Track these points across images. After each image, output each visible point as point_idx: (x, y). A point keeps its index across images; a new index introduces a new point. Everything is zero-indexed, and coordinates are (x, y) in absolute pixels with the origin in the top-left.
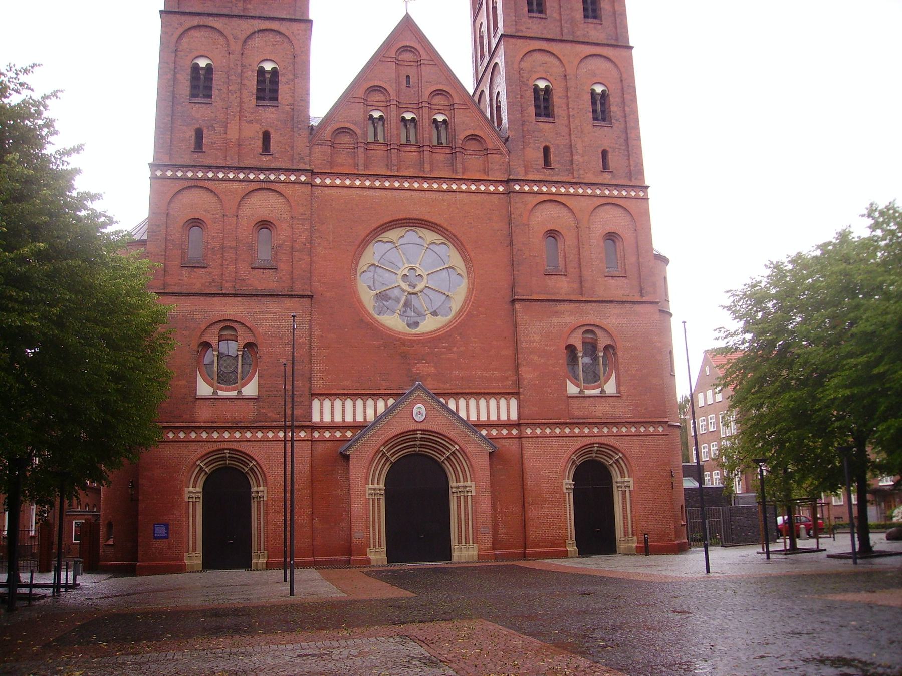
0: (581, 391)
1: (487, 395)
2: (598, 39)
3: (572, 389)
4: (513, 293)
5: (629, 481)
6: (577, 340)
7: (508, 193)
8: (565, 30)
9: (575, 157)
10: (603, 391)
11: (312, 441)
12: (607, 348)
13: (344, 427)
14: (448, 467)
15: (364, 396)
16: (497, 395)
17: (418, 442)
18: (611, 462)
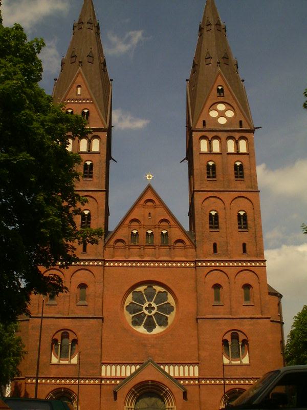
0: (230, 362)
1: (184, 364)
3: (226, 361)
6: (228, 337)
7: (196, 267)
10: (241, 362)
11: (101, 385)
13: (116, 379)
16: (189, 364)
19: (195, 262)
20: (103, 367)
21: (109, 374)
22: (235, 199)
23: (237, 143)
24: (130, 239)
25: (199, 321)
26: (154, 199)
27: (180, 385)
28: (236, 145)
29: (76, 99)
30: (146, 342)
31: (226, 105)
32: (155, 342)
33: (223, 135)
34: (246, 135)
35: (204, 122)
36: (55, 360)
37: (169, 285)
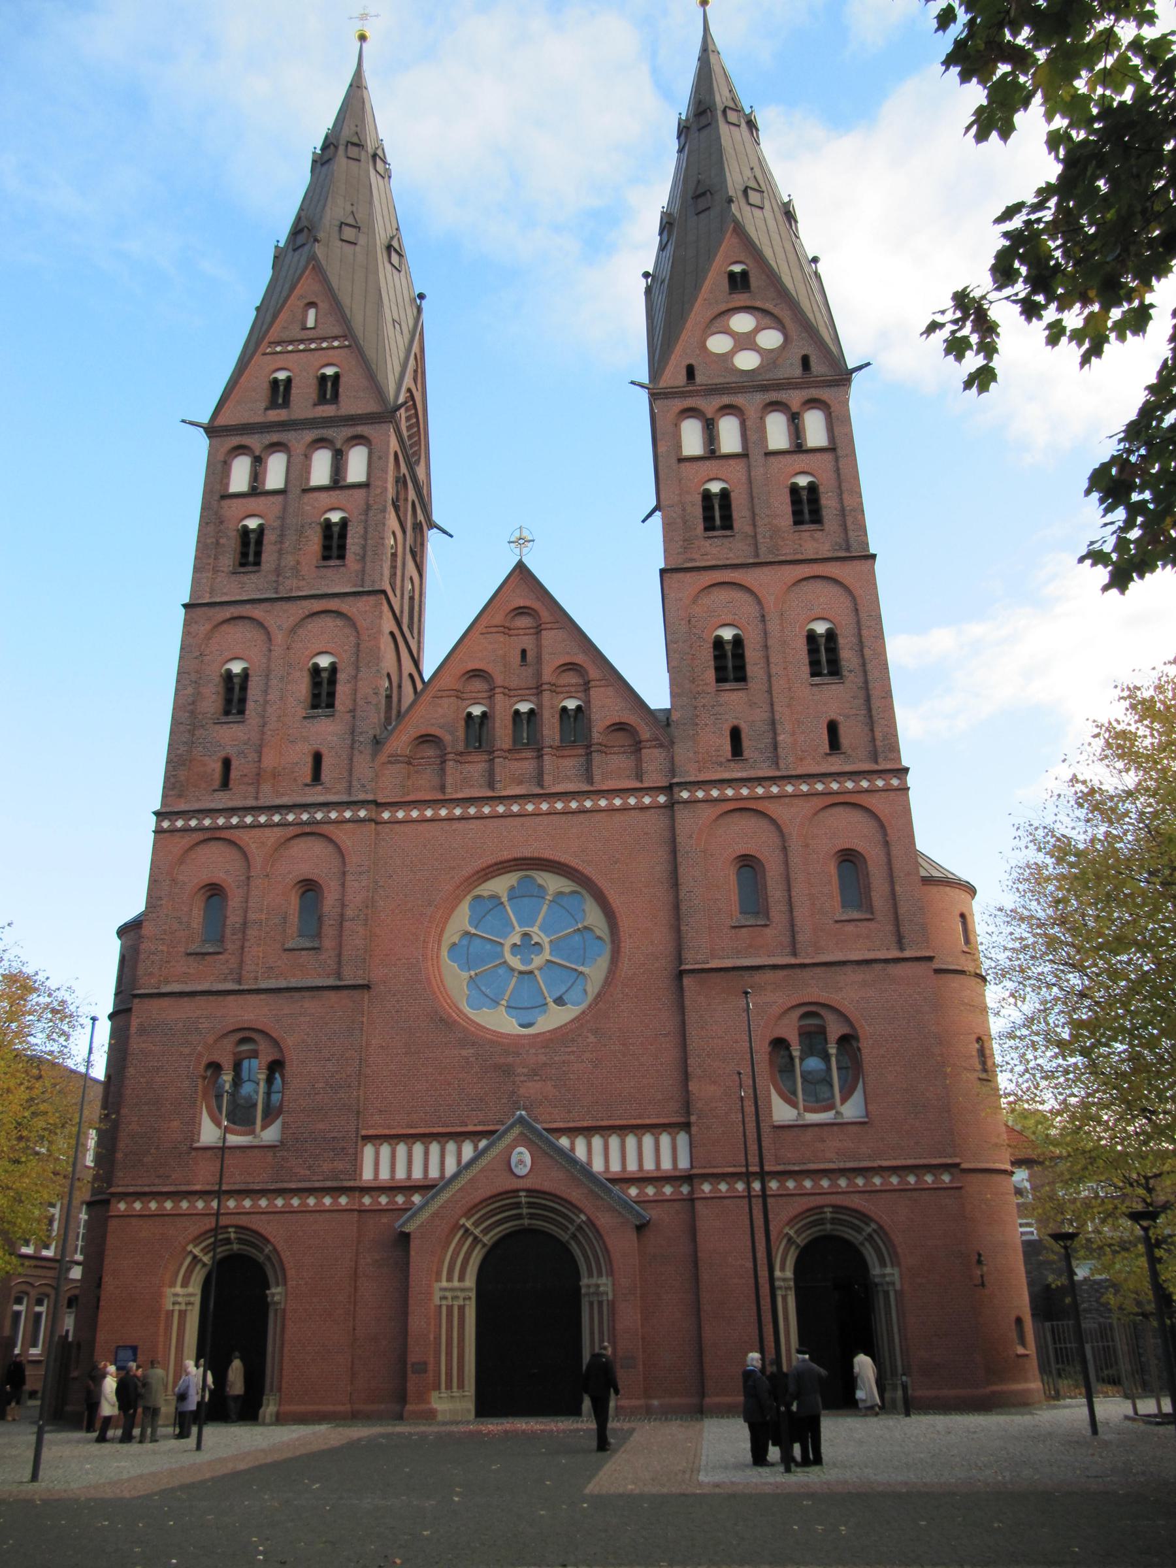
1: (638, 1129)
2: (817, 553)
3: (782, 1112)
4: (680, 959)
5: (893, 1274)
6: (789, 1030)
7: (671, 805)
8: (763, 550)
9: (781, 738)
12: (845, 1041)
13: (409, 1189)
15: (442, 1137)
16: (655, 1129)
17: (525, 1211)
18: (861, 1238)
19: (669, 789)
20: (368, 1151)
22: (794, 584)
23: (795, 420)
24: (461, 733)
25: (687, 981)
26: (536, 605)
27: (625, 1204)
28: (792, 428)
29: (302, 341)
30: (510, 1059)
31: (759, 314)
32: (543, 1059)
33: (751, 403)
35: (690, 372)
36: (209, 1133)
37: (588, 870)
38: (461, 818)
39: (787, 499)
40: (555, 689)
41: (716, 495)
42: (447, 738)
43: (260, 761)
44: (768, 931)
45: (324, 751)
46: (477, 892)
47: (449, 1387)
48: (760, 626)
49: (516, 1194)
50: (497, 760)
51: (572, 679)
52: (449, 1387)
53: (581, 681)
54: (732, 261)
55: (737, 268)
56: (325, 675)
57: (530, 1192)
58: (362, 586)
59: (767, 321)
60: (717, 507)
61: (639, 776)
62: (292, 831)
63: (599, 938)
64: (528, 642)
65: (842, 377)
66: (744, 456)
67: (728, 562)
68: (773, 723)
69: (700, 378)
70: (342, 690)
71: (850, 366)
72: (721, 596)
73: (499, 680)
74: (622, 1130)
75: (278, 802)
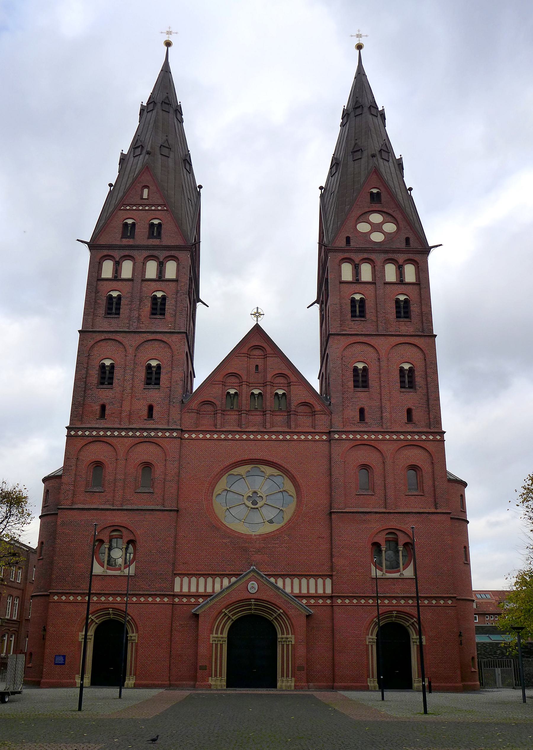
1: (308, 576)
8: (380, 328)
13: (197, 596)
14: (276, 623)
15: (213, 576)
21: (185, 590)
25: (333, 516)
28: (398, 272)
33: (379, 258)
34: (417, 257)
38: (225, 440)
39: (393, 305)
40: (272, 384)
41: (357, 301)
42: (218, 403)
43: (121, 407)
44: (373, 497)
45: (154, 404)
46: (231, 472)
47: (216, 676)
48: (377, 363)
49: (250, 600)
50: (243, 415)
51: (282, 380)
52: (216, 676)
53: (286, 382)
54: (372, 187)
55: (375, 191)
56: (154, 369)
57: (256, 600)
58: (174, 329)
59: (389, 218)
60: (357, 306)
61: (314, 427)
62: (138, 440)
63: (290, 495)
64: (260, 362)
65: (426, 250)
66: (373, 283)
67: (363, 333)
68: (381, 407)
69: (352, 244)
70: (164, 377)
71: (430, 245)
72: (358, 348)
73: (245, 378)
74: (300, 576)
75: (131, 426)
